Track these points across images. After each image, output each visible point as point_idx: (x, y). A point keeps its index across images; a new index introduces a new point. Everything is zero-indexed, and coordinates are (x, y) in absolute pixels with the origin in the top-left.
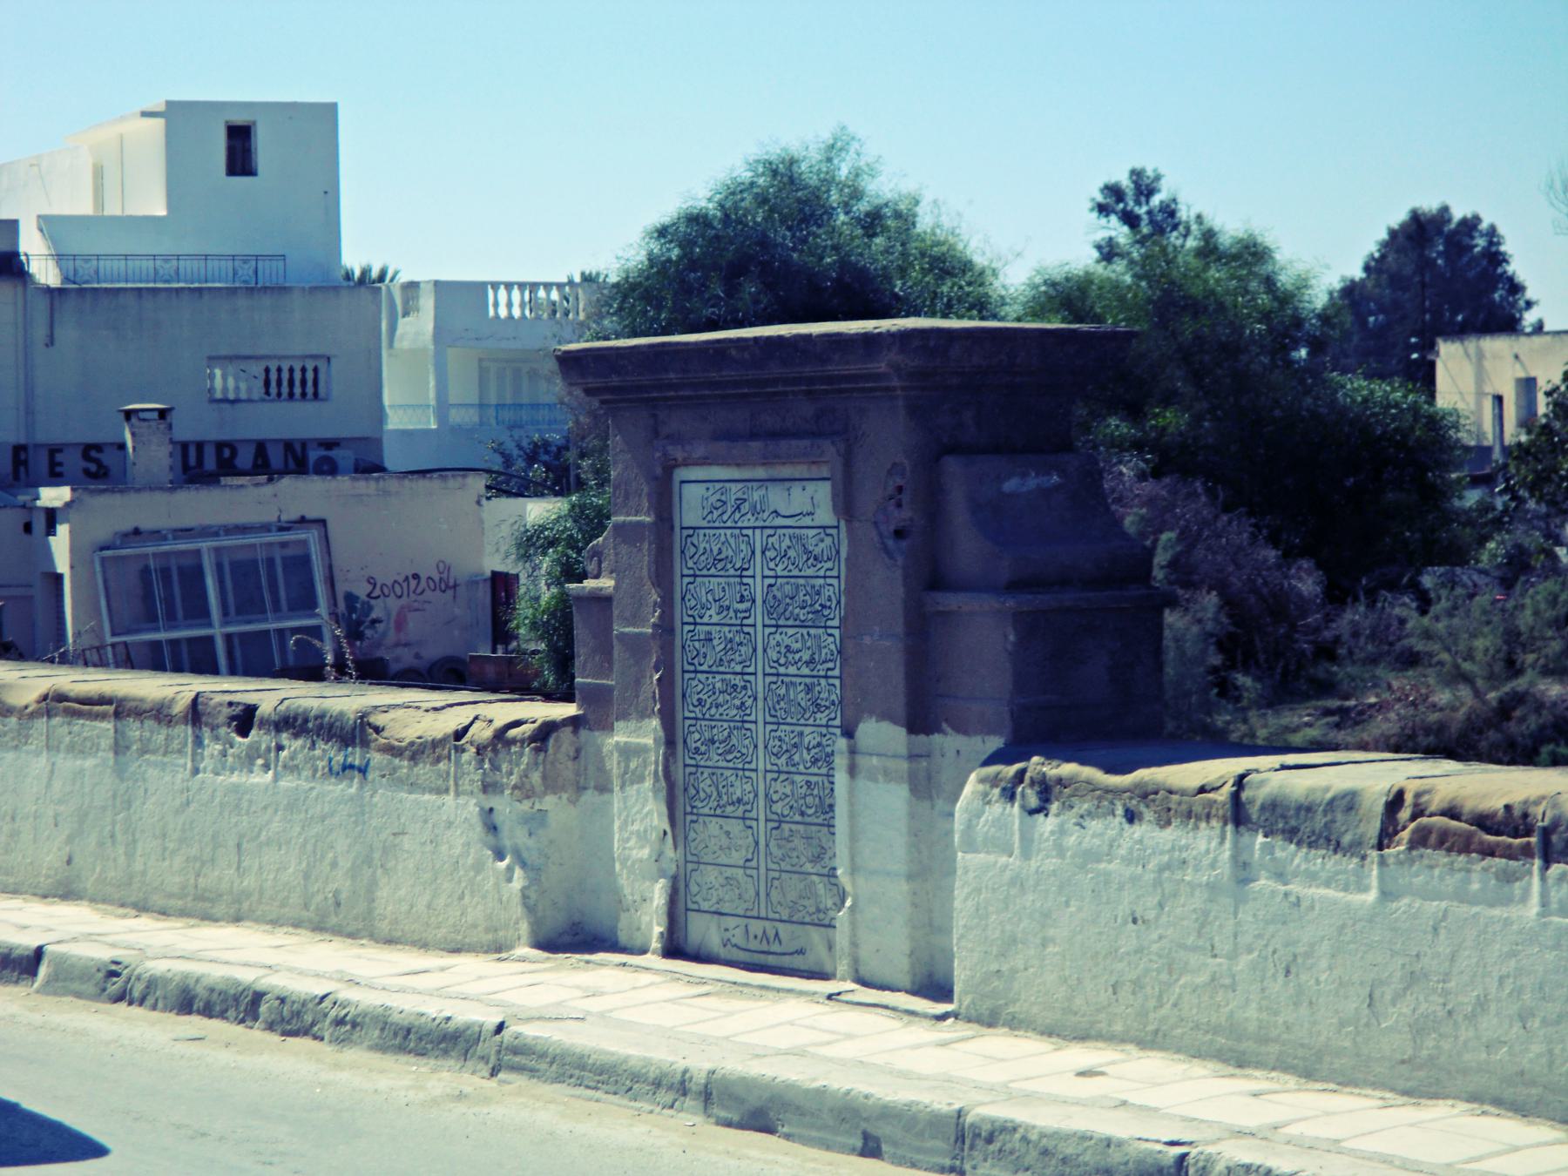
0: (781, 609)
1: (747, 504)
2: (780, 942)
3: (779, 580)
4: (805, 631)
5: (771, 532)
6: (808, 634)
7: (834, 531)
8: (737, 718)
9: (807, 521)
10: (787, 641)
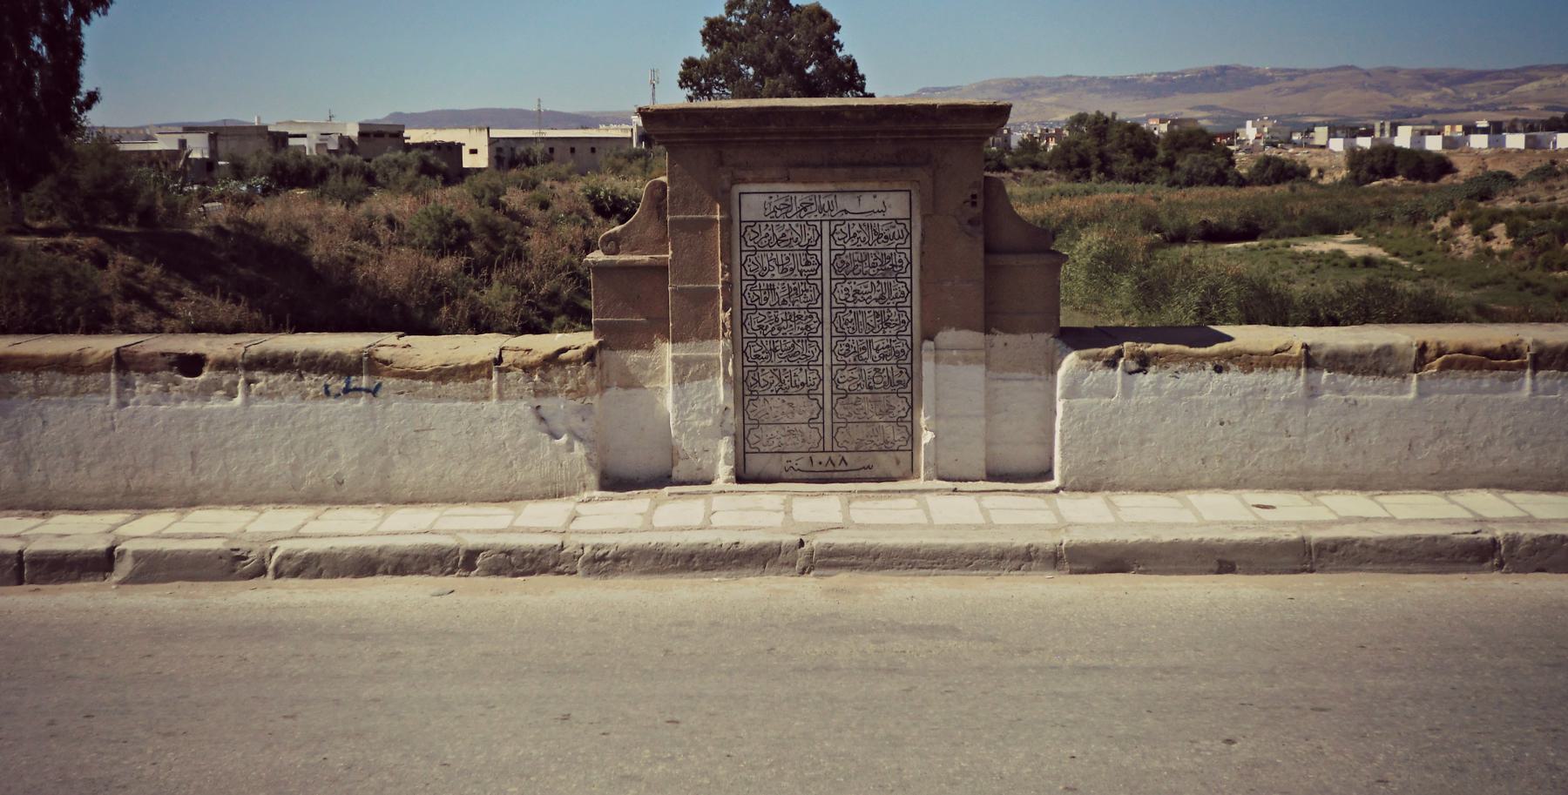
0: (851, 268)
1: (814, 207)
2: (846, 464)
4: (875, 282)
9: (880, 216)
10: (854, 287)
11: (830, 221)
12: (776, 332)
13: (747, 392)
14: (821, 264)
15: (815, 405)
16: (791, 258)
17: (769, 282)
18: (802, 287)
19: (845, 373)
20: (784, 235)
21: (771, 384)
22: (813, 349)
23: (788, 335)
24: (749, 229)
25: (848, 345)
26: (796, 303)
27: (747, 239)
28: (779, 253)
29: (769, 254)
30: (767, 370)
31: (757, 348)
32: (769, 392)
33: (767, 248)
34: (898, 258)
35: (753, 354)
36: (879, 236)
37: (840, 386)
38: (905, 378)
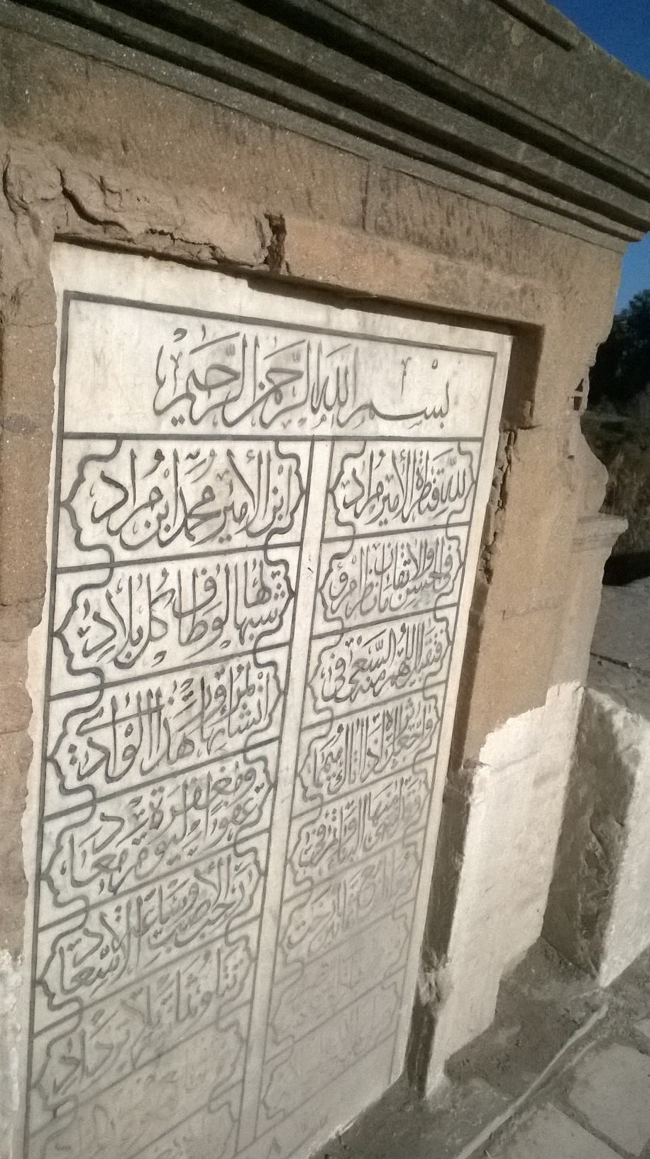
1: (301, 385)
3: (363, 543)
4: (396, 626)
5: (354, 447)
6: (403, 629)
7: (473, 447)
8: (224, 842)
9: (430, 428)
11: (335, 439)
14: (293, 594)
16: (221, 580)
17: (143, 687)
18: (240, 684)
19: (307, 914)
20: (209, 492)
21: (120, 1046)
22: (244, 876)
23: (186, 859)
24: (93, 471)
25: (323, 830)
26: (216, 744)
27: (84, 520)
28: (187, 567)
29: (155, 571)
31: (87, 943)
32: (104, 1082)
33: (153, 550)
34: (446, 553)
35: (71, 972)
36: (423, 485)
37: (293, 954)
38: (412, 865)
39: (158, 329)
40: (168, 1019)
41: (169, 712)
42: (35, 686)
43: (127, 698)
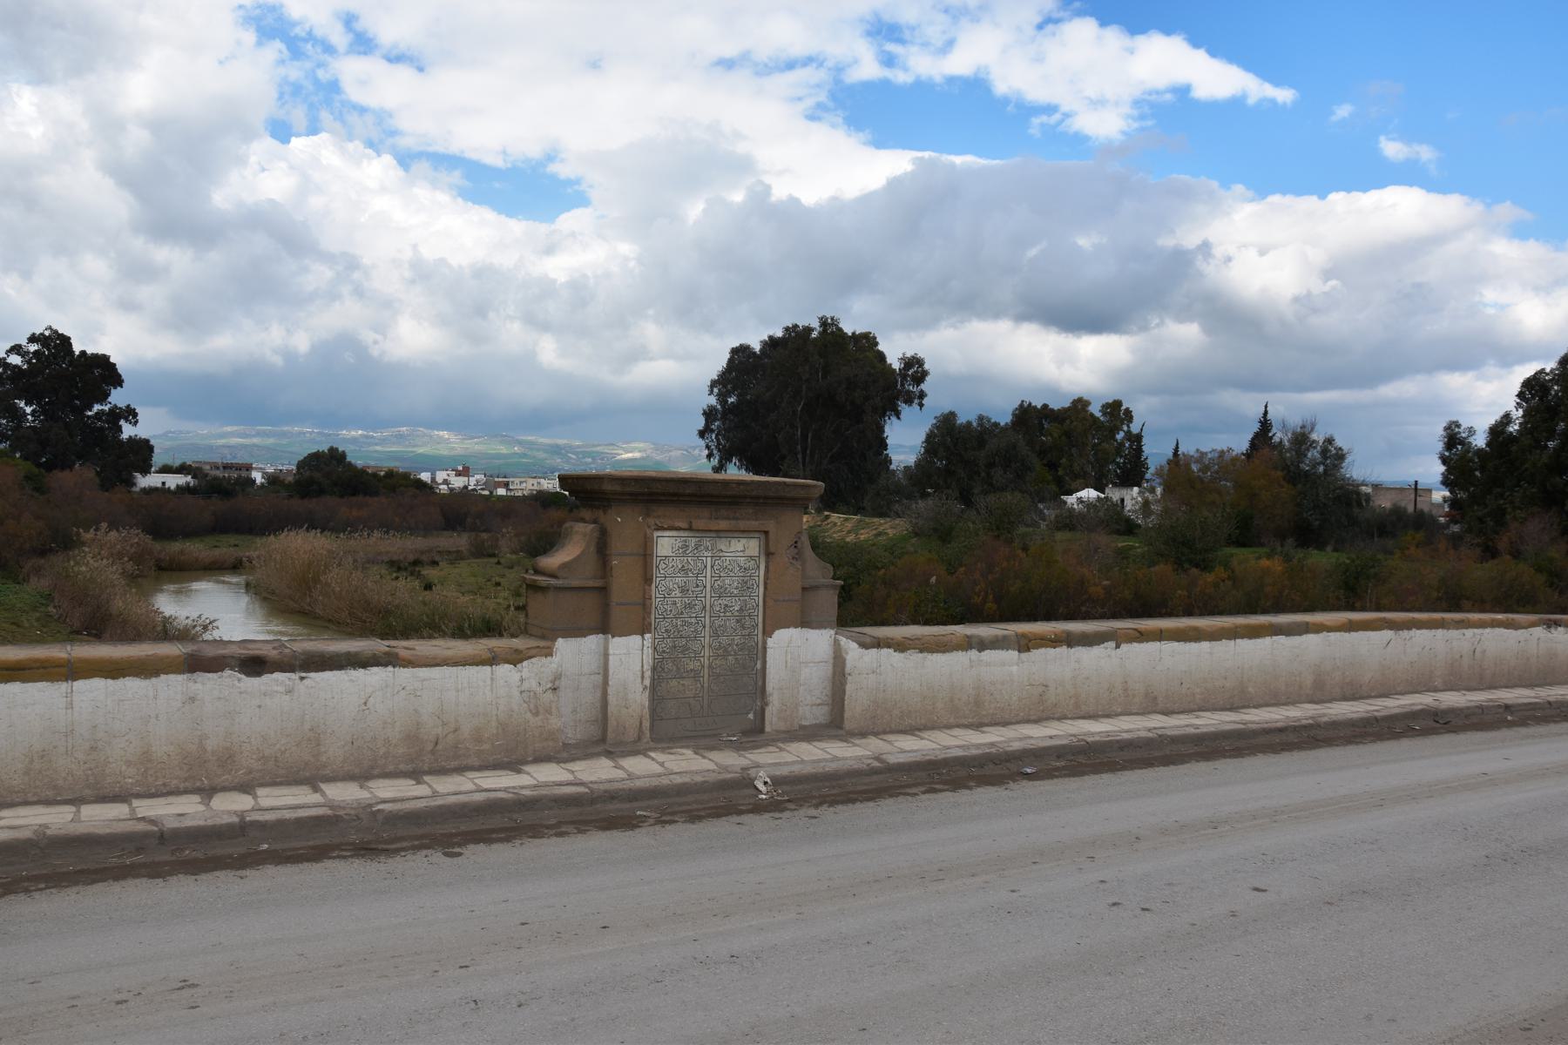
4: (737, 598)
7: (757, 559)
9: (741, 554)
10: (726, 603)
12: (676, 633)
13: (656, 677)
14: (705, 587)
15: (699, 685)
28: (680, 579)
30: (669, 661)
36: (741, 567)
39: (673, 540)
40: (682, 670)
41: (678, 605)
42: (653, 596)
43: (670, 601)
